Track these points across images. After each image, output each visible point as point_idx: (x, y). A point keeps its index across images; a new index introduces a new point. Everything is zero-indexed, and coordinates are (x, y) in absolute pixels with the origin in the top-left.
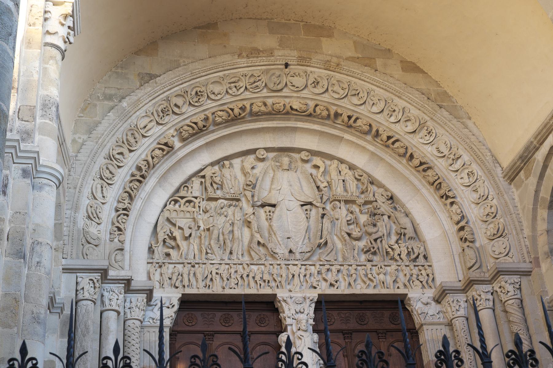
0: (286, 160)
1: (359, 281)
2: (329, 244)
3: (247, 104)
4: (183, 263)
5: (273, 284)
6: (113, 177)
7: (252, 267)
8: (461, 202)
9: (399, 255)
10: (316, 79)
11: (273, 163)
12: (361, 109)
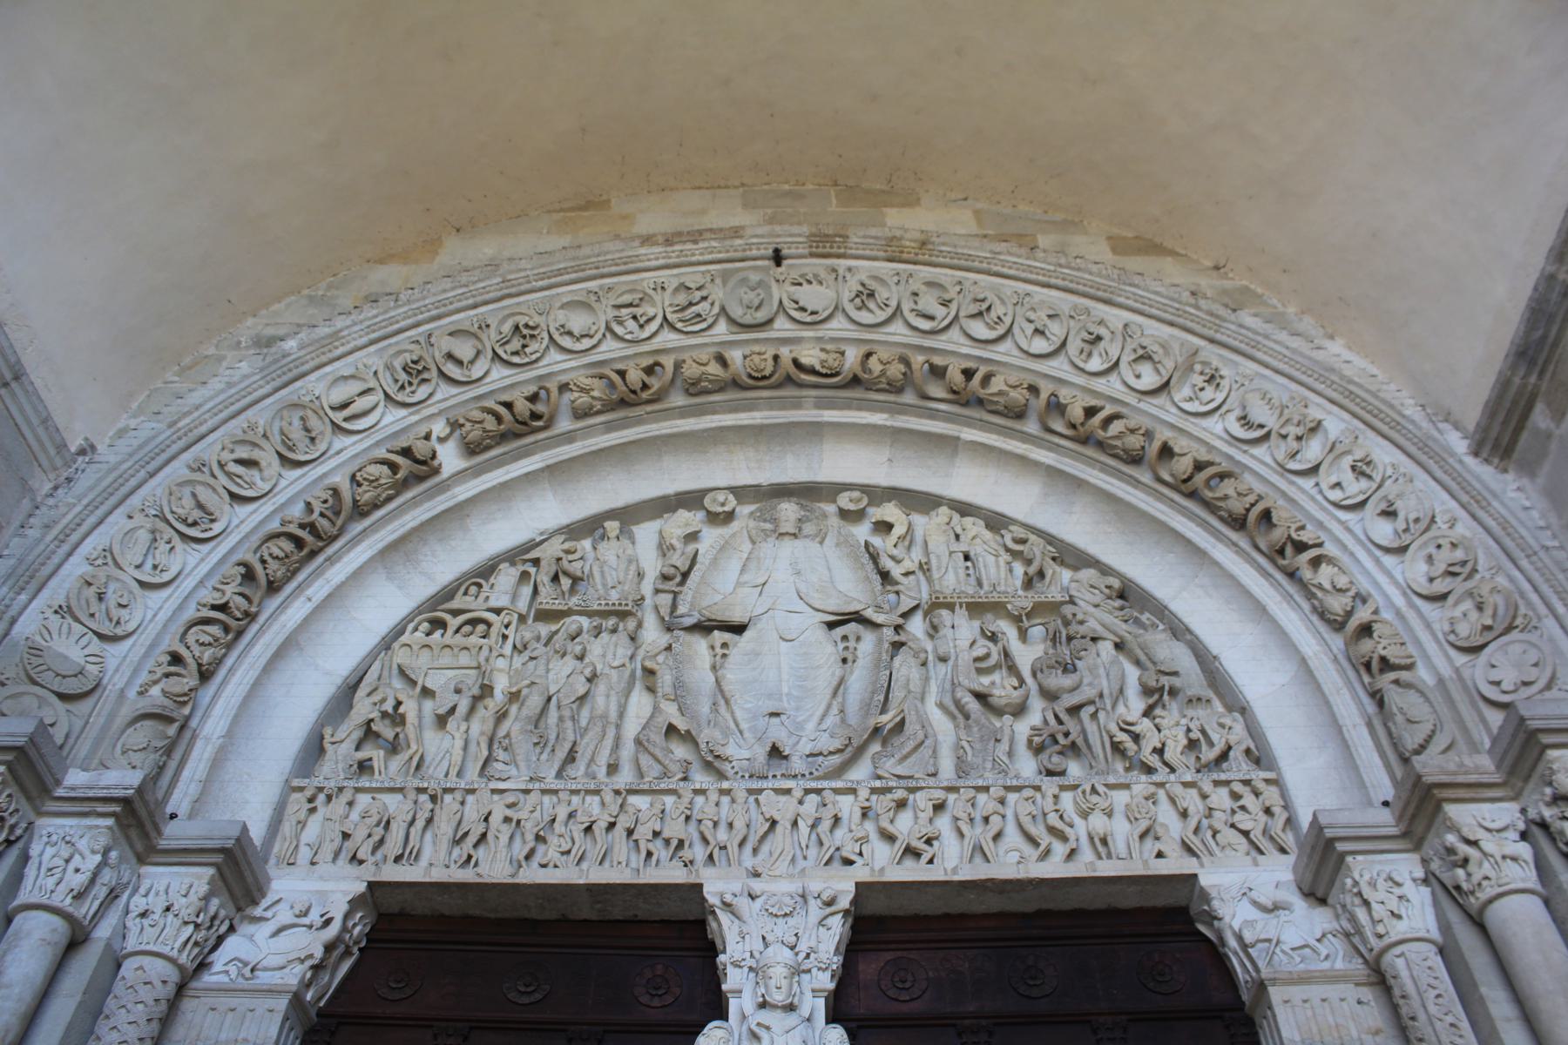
0: (788, 510)
2: (910, 728)
3: (668, 362)
4: (401, 790)
5: (699, 853)
6: (212, 521)
7: (633, 800)
9: (1160, 751)
10: (863, 285)
11: (752, 524)
12: (1004, 352)
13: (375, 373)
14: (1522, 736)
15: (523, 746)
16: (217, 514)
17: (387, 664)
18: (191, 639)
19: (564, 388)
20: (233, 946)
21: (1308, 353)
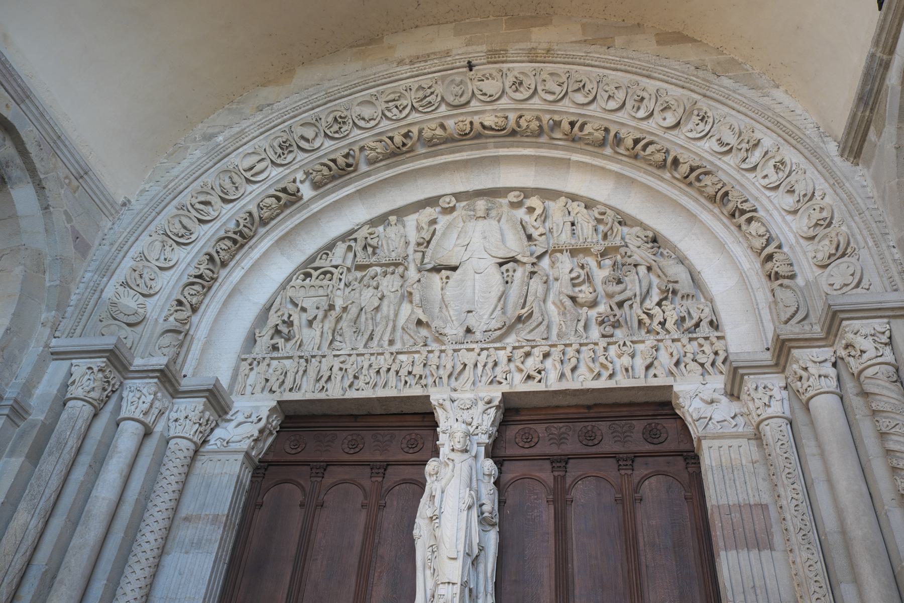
0: (481, 204)
1: (582, 369)
2: (535, 316)
3: (415, 130)
4: (291, 358)
6: (191, 234)
7: (402, 357)
8: (768, 218)
9: (663, 324)
10: (516, 78)
11: (464, 212)
13: (265, 150)
14: (830, 314)
15: (348, 331)
16: (193, 230)
17: (284, 297)
18: (186, 293)
19: (362, 149)
20: (218, 432)
21: (756, 99)
